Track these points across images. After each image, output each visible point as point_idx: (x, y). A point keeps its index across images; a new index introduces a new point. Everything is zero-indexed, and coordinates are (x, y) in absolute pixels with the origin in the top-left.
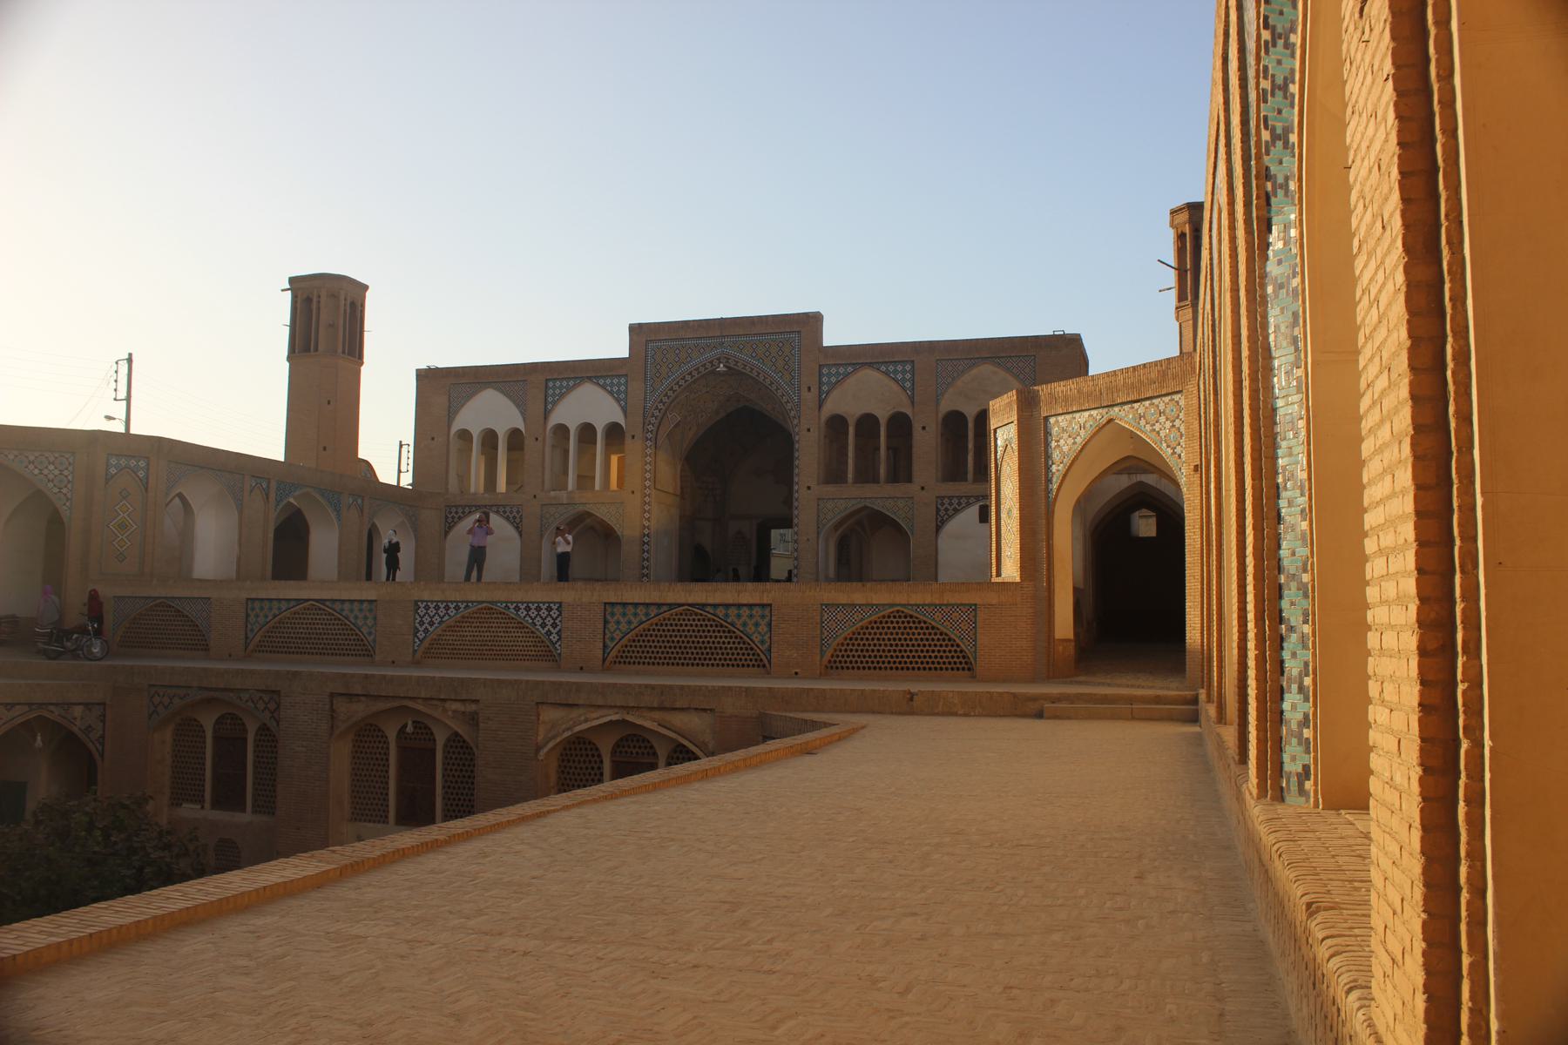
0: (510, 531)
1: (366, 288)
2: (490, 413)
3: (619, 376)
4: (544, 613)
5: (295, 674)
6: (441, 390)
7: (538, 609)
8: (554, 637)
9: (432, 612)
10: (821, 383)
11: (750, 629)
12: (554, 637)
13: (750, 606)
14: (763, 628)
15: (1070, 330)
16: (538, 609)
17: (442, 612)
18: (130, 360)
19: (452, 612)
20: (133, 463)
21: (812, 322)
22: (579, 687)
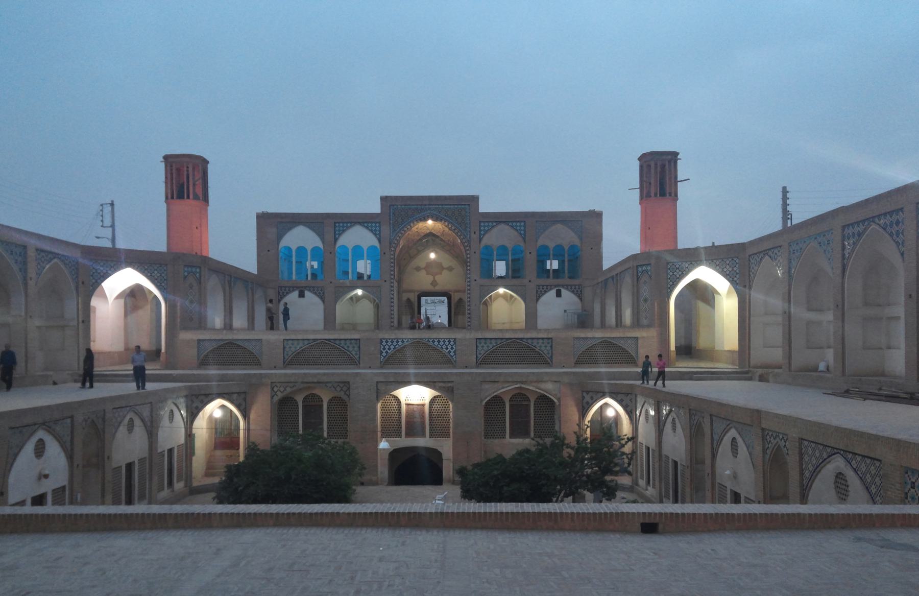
0: (317, 300)
1: (207, 162)
2: (301, 238)
3: (376, 223)
4: (447, 343)
5: (357, 374)
6: (272, 226)
7: (444, 341)
8: (452, 354)
9: (390, 343)
10: (480, 230)
11: (543, 348)
12: (452, 354)
13: (543, 339)
14: (549, 348)
15: (597, 209)
16: (444, 341)
17: (395, 343)
18: (112, 204)
19: (400, 343)
20: (194, 270)
21: (475, 199)
22: (500, 374)
